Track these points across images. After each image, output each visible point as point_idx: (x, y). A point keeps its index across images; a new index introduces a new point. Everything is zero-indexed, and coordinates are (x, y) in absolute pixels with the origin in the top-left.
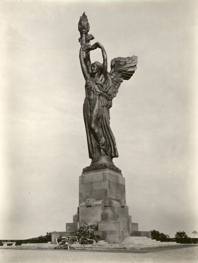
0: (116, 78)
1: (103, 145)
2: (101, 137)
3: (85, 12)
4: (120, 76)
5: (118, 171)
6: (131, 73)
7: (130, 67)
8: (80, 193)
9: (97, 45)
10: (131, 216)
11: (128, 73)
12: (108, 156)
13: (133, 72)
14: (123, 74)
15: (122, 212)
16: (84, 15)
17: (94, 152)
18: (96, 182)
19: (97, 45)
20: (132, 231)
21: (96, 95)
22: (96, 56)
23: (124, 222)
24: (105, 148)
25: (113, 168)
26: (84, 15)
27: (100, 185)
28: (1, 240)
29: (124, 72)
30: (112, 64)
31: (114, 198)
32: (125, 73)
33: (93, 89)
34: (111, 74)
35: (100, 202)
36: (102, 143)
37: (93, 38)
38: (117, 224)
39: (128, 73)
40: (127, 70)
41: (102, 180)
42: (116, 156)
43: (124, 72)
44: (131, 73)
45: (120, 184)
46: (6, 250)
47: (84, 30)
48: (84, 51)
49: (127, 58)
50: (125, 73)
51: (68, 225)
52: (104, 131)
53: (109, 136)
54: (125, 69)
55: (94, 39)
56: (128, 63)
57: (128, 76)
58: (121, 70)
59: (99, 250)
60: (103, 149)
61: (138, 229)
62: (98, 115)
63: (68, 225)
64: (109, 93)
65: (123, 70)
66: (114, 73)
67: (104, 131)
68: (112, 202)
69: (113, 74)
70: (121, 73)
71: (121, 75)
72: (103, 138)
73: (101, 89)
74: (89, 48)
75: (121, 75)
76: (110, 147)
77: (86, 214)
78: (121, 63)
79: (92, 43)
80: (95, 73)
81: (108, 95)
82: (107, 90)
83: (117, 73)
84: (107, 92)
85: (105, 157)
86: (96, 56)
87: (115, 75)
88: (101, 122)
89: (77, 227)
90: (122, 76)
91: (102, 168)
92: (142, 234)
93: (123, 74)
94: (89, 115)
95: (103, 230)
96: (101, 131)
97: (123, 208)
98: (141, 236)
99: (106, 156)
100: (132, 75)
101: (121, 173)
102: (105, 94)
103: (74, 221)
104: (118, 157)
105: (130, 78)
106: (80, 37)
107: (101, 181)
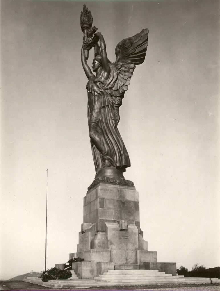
0: (124, 66)
1: (107, 154)
3: (85, 6)
4: (129, 63)
5: (130, 184)
6: (144, 52)
7: (138, 46)
10: (147, 242)
11: (138, 55)
12: (114, 167)
13: (145, 50)
14: (132, 59)
15: (121, 237)
20: (140, 262)
21: (95, 95)
23: (127, 250)
24: (110, 158)
25: (116, 181)
29: (132, 56)
31: (113, 219)
32: (134, 56)
34: (116, 65)
36: (105, 153)
38: (104, 253)
39: (138, 55)
40: (135, 52)
43: (132, 56)
44: (144, 52)
45: (127, 201)
47: (85, 26)
48: (85, 50)
49: (134, 36)
50: (134, 56)
52: (106, 136)
53: (113, 141)
54: (133, 51)
56: (135, 42)
58: (127, 55)
60: (108, 160)
61: (156, 259)
62: (97, 119)
64: (114, 89)
65: (133, 53)
66: (120, 61)
67: (106, 136)
68: (105, 225)
69: (119, 63)
70: (128, 58)
71: (129, 61)
73: (100, 87)
74: (90, 43)
75: (129, 61)
76: (115, 155)
78: (125, 47)
81: (113, 91)
82: (109, 86)
83: (123, 60)
84: (111, 88)
85: (110, 168)
87: (121, 64)
90: (131, 61)
92: (151, 266)
93: (132, 59)
96: (103, 139)
97: (123, 232)
98: (150, 269)
99: (112, 166)
100: (145, 54)
101: (134, 187)
102: (108, 91)
104: (130, 166)
105: (144, 58)
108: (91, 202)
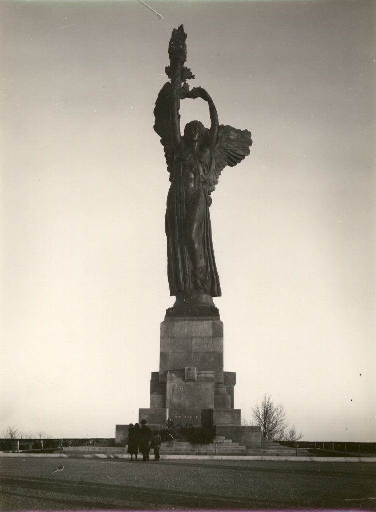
2: (201, 258)
8: (161, 353)
9: (200, 93)
16: (181, 28)
17: (187, 282)
18: (198, 337)
19: (200, 93)
22: (191, 111)
26: (181, 28)
27: (208, 344)
28: (69, 439)
30: (219, 135)
33: (195, 169)
35: (210, 374)
37: (192, 77)
41: (211, 335)
42: (219, 294)
43: (231, 153)
46: (130, 464)
51: (142, 411)
55: (194, 78)
57: (234, 160)
59: (286, 461)
63: (142, 411)
72: (203, 260)
75: (226, 156)
77: (182, 394)
79: (192, 84)
80: (196, 141)
83: (222, 151)
86: (191, 111)
88: (203, 232)
89: (165, 417)
91: (210, 315)
94: (185, 213)
95: (222, 424)
100: (239, 160)
103: (151, 404)
106: (168, 63)
107: (209, 338)
108: (192, 338)
